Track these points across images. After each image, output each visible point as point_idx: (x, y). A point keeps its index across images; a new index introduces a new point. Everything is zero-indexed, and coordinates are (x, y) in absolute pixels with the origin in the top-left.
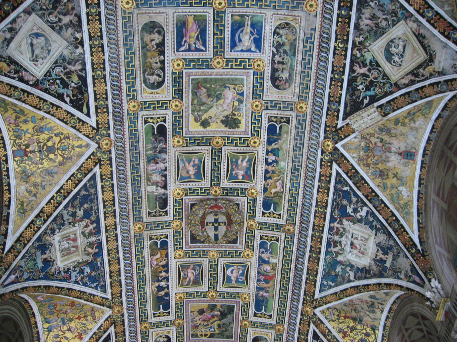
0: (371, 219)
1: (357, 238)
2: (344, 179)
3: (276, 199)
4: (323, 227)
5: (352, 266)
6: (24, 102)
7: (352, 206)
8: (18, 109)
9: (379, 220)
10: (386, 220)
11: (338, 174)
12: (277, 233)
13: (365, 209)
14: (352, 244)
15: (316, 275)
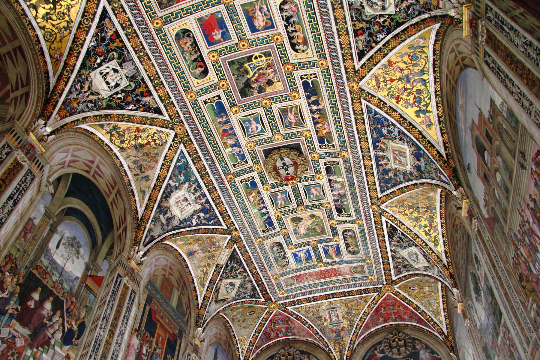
0: (188, 223)
1: (187, 206)
2: (216, 225)
3: (249, 190)
4: (210, 193)
5: (177, 188)
6: (424, 242)
7: (202, 218)
8: (428, 237)
9: (184, 227)
10: (181, 232)
11: (221, 225)
12: (237, 170)
13: (195, 223)
14: (186, 200)
15: (193, 160)
